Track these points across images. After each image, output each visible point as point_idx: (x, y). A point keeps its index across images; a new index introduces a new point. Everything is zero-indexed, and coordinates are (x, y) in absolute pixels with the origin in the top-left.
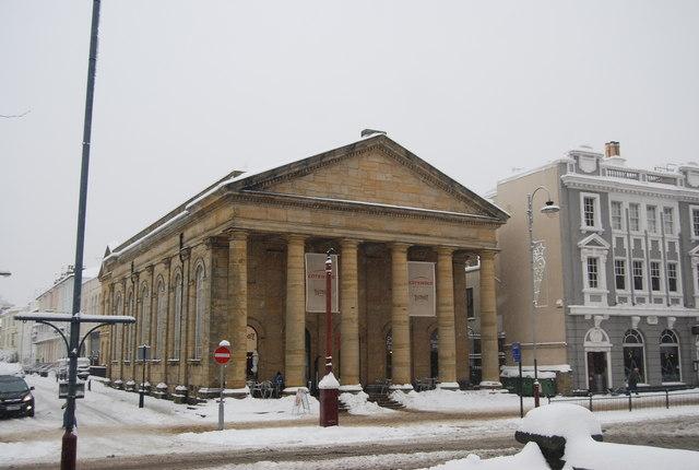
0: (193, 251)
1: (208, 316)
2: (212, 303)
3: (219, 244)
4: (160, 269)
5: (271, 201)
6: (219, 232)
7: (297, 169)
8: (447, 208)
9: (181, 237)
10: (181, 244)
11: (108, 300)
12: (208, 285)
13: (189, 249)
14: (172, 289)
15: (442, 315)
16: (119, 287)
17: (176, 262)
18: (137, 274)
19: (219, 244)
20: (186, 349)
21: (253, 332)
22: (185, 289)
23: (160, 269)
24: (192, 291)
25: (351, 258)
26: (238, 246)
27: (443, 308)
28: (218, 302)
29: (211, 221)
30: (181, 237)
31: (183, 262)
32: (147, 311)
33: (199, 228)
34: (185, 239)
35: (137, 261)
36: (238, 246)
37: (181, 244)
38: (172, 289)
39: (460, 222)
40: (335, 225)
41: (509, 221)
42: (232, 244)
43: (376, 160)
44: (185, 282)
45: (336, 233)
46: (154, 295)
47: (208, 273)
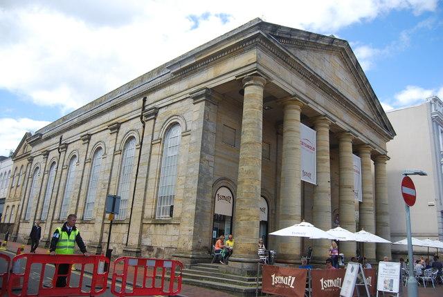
0: (161, 111)
2: (201, 157)
5: (285, 59)
9: (144, 100)
10: (144, 107)
22: (145, 149)
26: (253, 95)
27: (366, 195)
28: (207, 157)
30: (144, 100)
34: (147, 103)
35: (65, 135)
36: (253, 95)
40: (320, 102)
42: (248, 91)
45: (320, 110)
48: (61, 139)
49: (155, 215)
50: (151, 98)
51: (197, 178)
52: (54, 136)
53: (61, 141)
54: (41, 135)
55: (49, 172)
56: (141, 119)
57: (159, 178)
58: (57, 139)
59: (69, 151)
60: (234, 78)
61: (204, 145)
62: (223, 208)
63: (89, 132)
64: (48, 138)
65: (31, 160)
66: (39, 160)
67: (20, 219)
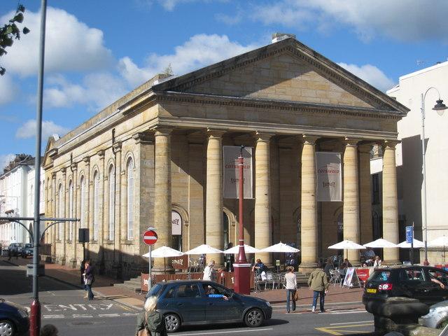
1: (138, 202)
2: (141, 191)
3: (146, 138)
4: (95, 160)
6: (145, 128)
7: (214, 71)
8: (353, 101)
9: (113, 132)
10: (114, 138)
11: (51, 186)
12: (137, 174)
13: (120, 143)
14: (106, 178)
15: (346, 200)
16: (60, 175)
17: (109, 154)
18: (76, 164)
19: (146, 138)
20: (120, 231)
21: (179, 218)
23: (95, 160)
24: (123, 180)
25: (261, 150)
26: (160, 140)
29: (139, 118)
30: (113, 132)
31: (115, 153)
32: (84, 197)
33: (129, 124)
34: (116, 135)
35: (76, 152)
36: (160, 140)
37: (114, 138)
38: (106, 178)
39: (364, 115)
41: (409, 113)
43: (286, 60)
44: (118, 172)
46: (91, 184)
47: (138, 165)
48: (71, 157)
49: (127, 237)
50: (119, 129)
51: (139, 209)
52: (67, 152)
53: (71, 159)
54: (57, 150)
55: (69, 190)
56: (113, 149)
57: (127, 206)
58: (67, 156)
59: (79, 171)
60: (147, 128)
61: (143, 181)
62: (176, 230)
63: (90, 154)
64: (63, 154)
65: (54, 175)
66: (60, 175)
67: (55, 239)
